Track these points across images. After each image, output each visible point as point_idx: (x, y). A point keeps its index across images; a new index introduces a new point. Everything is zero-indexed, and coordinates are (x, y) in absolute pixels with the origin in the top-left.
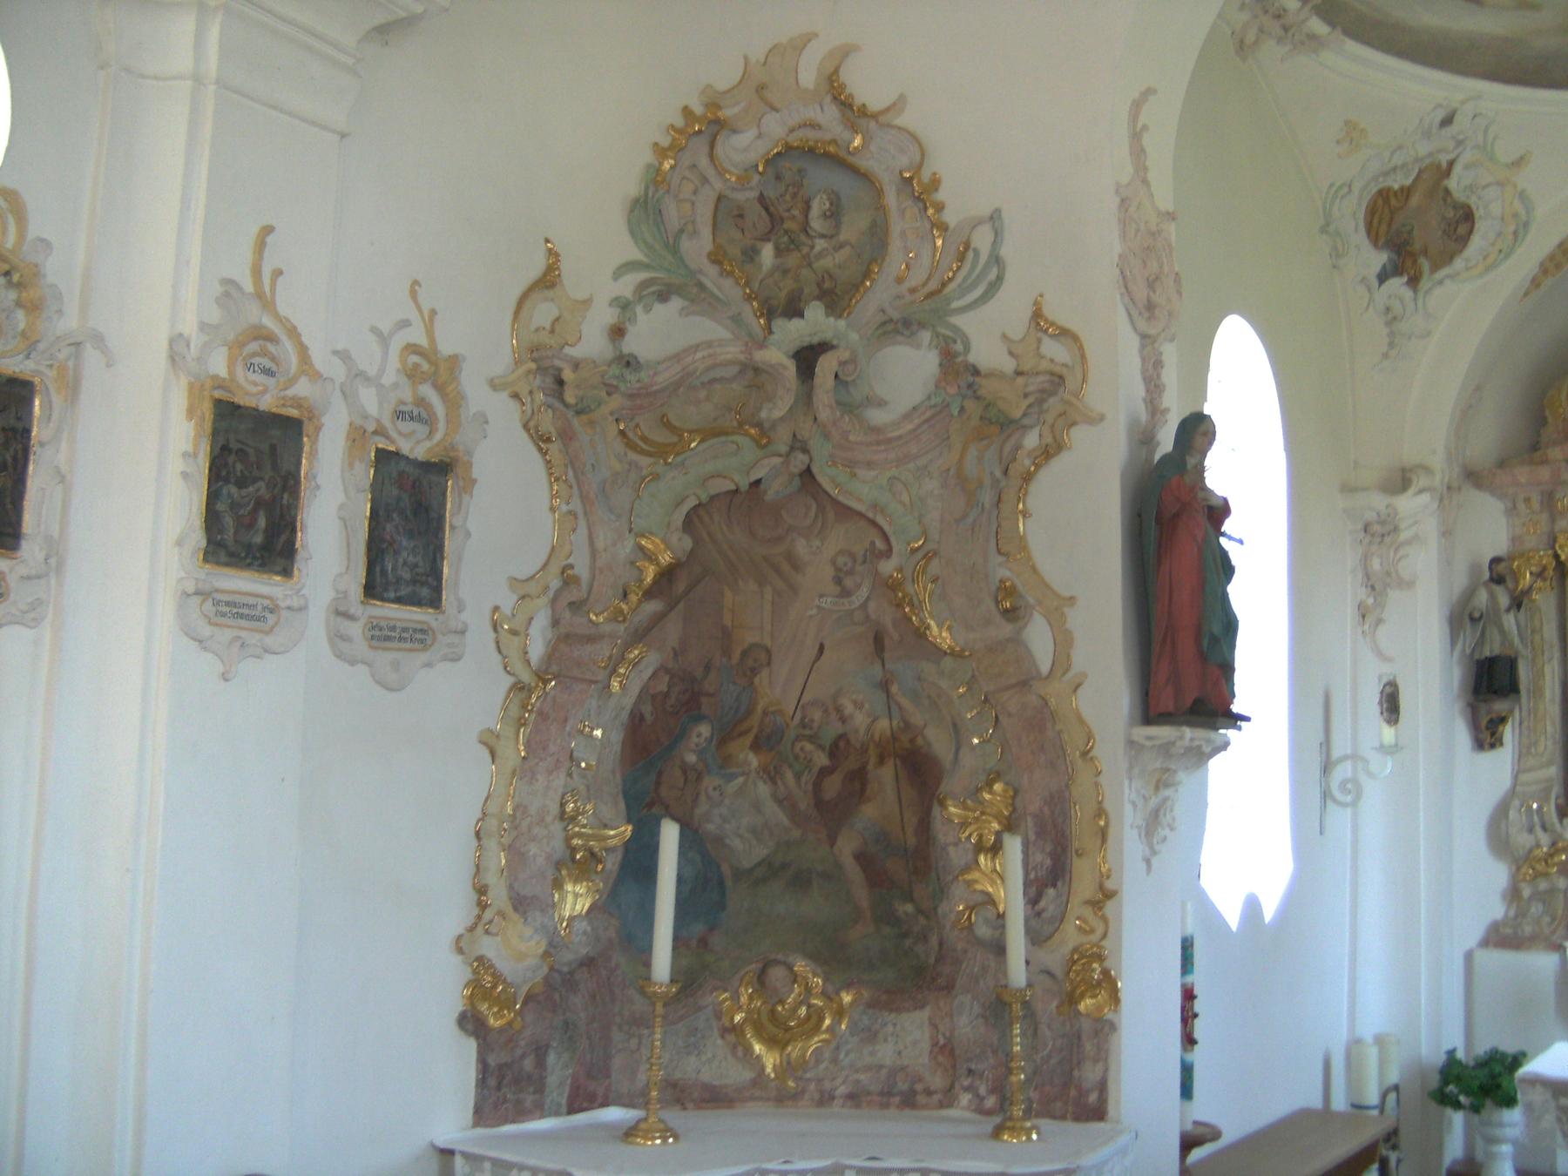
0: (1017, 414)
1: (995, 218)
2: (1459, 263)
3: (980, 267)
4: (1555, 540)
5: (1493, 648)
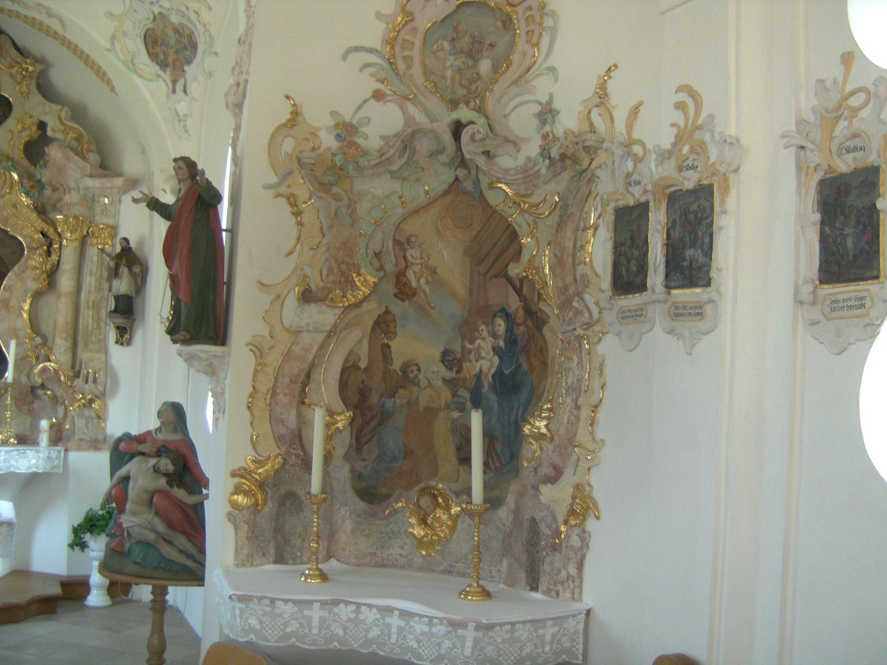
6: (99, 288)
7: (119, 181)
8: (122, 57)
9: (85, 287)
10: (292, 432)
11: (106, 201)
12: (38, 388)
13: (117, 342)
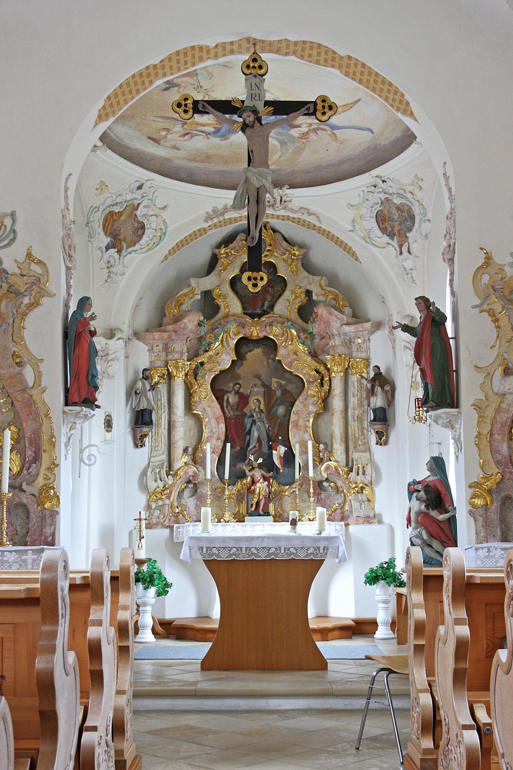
0: (22, 291)
1: (13, 215)
2: (138, 246)
3: (7, 233)
4: (167, 363)
5: (144, 405)
6: (361, 405)
7: (368, 325)
8: (362, 235)
9: (351, 406)
10: (506, 457)
11: (360, 341)
12: (324, 481)
13: (377, 444)
